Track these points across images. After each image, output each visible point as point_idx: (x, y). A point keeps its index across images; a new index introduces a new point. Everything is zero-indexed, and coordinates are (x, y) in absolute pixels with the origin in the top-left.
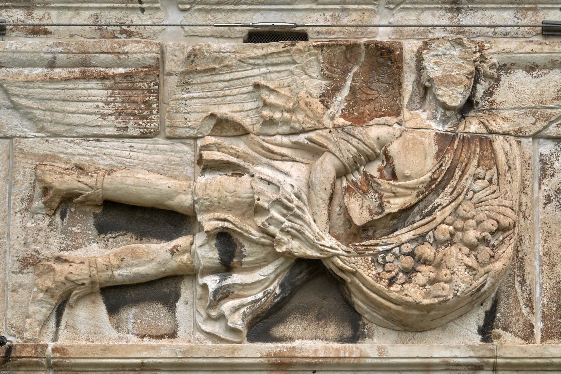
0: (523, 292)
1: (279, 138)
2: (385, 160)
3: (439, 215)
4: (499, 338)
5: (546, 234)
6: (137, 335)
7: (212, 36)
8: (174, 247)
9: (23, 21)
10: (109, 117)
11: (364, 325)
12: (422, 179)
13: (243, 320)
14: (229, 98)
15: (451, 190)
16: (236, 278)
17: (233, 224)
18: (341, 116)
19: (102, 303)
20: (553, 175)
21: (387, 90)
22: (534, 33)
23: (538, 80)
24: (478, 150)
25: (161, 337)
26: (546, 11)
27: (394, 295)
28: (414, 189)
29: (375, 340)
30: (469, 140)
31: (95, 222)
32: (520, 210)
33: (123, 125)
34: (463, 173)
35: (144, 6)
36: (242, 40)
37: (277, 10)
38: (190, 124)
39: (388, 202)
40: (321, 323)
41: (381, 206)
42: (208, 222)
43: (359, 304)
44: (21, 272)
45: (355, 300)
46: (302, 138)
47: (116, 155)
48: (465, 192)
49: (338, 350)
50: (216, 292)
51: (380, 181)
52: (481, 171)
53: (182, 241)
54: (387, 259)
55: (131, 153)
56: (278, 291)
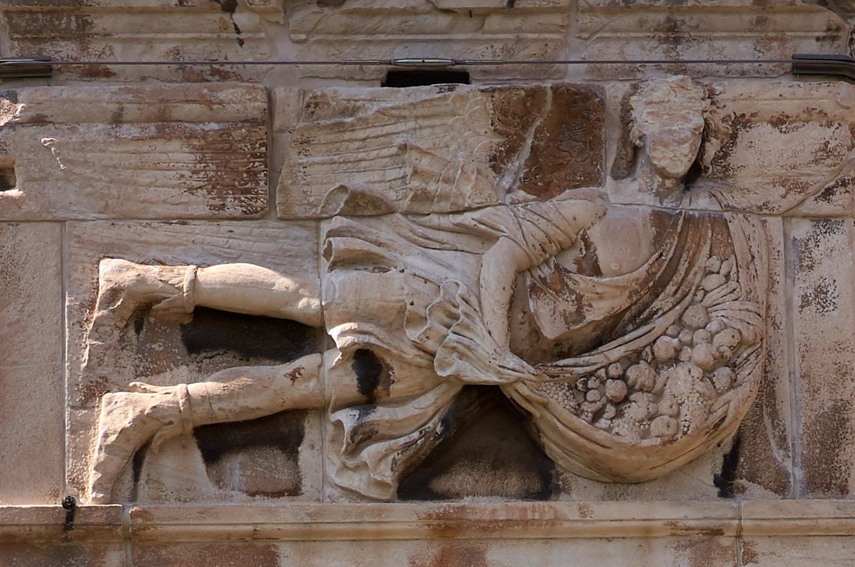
0: (774, 428)
1: (435, 220)
2: (583, 247)
3: (659, 323)
4: (744, 492)
6: (246, 492)
7: (337, 77)
8: (295, 371)
9: (75, 59)
10: (199, 190)
11: (558, 474)
12: (635, 274)
13: (392, 469)
14: (363, 164)
15: (674, 288)
16: (380, 414)
17: (378, 338)
18: (519, 188)
19: (197, 448)
20: (811, 267)
22: (782, 72)
23: (787, 137)
25: (279, 494)
26: (796, 41)
27: (601, 435)
28: (625, 288)
29: (574, 496)
32: (767, 316)
33: (218, 202)
35: (242, 36)
36: (379, 83)
38: (312, 199)
39: (590, 306)
40: (498, 473)
41: (579, 313)
43: (553, 449)
45: (545, 440)
46: (467, 219)
47: (209, 244)
48: (693, 291)
49: (525, 509)
50: (354, 432)
51: (577, 277)
52: (714, 262)
53: (306, 362)
55: (230, 241)
56: (439, 429)
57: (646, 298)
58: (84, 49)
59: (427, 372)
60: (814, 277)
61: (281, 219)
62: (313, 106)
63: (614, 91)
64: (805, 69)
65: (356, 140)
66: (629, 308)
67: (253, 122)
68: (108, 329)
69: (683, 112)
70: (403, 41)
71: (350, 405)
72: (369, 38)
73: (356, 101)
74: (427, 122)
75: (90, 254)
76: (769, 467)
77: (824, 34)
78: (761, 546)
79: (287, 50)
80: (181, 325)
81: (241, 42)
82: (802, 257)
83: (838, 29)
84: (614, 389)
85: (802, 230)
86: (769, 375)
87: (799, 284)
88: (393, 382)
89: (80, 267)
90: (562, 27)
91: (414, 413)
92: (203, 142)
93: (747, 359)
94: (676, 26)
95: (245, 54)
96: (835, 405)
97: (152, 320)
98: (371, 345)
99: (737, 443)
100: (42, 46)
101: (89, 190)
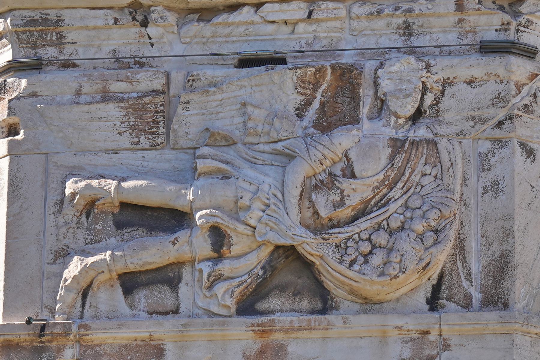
2: (346, 161)
3: (393, 207)
4: (444, 308)
5: (484, 219)
6: (147, 312)
8: (175, 239)
9: (56, 58)
11: (332, 298)
14: (221, 115)
17: (222, 219)
20: (489, 170)
21: (350, 103)
23: (476, 91)
24: (425, 150)
25: (166, 313)
26: (483, 32)
30: (418, 142)
31: (113, 220)
33: (136, 140)
34: (413, 171)
35: (152, 41)
36: (233, 66)
37: (262, 40)
38: (190, 136)
39: (349, 196)
40: (297, 298)
44: (54, 262)
46: (279, 146)
47: (131, 165)
48: (414, 186)
49: (310, 320)
51: (341, 180)
52: (428, 169)
54: (348, 245)
55: (143, 163)
56: (261, 273)
57: (385, 191)
58: (61, 51)
59: (253, 239)
60: (490, 176)
61: (173, 149)
63: (370, 65)
64: (488, 48)
65: (216, 101)
66: (374, 197)
67: (157, 93)
68: (70, 217)
69: (408, 78)
70: (246, 41)
71: (209, 259)
72: (228, 39)
73: (217, 77)
74: (258, 89)
75: (62, 172)
76: (460, 292)
77: (500, 27)
80: (113, 214)
81: (152, 45)
82: (484, 163)
83: (508, 24)
84: (366, 247)
85: (485, 146)
86: (461, 236)
87: (482, 180)
88: (233, 245)
89: (55, 180)
90: (341, 28)
91: (246, 262)
92: (127, 105)
93: (445, 227)
94: (409, 26)
95: (154, 52)
96: (502, 254)
97: (96, 211)
98: (217, 223)
99: (441, 277)
100: (37, 50)
101: (61, 135)
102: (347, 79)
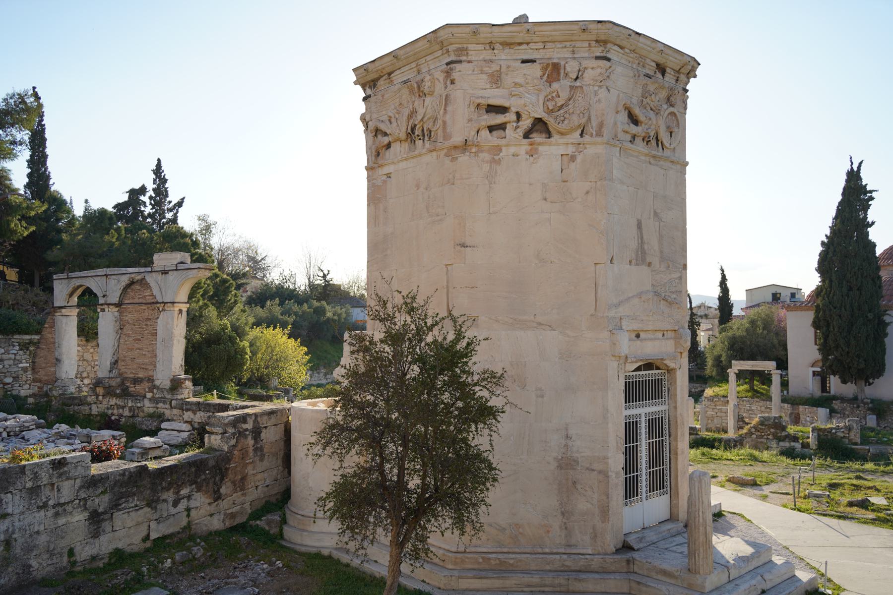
16: (520, 123)
42: (514, 109)
43: (551, 129)
62: (508, 67)
63: (562, 63)
64: (597, 58)
78: (588, 146)
79: (504, 57)
84: (562, 118)
85: (596, 88)
91: (526, 123)
95: (496, 58)
102: (556, 67)
